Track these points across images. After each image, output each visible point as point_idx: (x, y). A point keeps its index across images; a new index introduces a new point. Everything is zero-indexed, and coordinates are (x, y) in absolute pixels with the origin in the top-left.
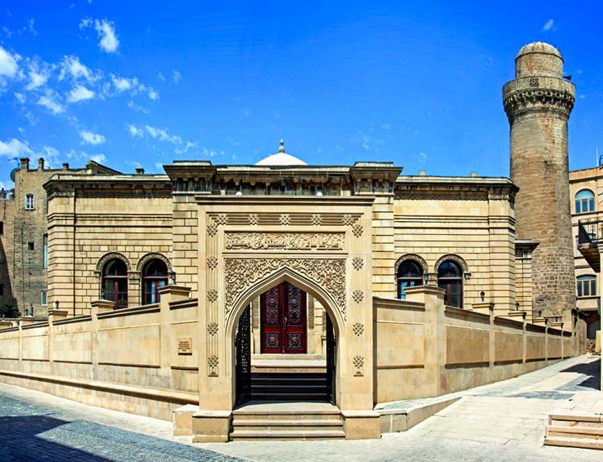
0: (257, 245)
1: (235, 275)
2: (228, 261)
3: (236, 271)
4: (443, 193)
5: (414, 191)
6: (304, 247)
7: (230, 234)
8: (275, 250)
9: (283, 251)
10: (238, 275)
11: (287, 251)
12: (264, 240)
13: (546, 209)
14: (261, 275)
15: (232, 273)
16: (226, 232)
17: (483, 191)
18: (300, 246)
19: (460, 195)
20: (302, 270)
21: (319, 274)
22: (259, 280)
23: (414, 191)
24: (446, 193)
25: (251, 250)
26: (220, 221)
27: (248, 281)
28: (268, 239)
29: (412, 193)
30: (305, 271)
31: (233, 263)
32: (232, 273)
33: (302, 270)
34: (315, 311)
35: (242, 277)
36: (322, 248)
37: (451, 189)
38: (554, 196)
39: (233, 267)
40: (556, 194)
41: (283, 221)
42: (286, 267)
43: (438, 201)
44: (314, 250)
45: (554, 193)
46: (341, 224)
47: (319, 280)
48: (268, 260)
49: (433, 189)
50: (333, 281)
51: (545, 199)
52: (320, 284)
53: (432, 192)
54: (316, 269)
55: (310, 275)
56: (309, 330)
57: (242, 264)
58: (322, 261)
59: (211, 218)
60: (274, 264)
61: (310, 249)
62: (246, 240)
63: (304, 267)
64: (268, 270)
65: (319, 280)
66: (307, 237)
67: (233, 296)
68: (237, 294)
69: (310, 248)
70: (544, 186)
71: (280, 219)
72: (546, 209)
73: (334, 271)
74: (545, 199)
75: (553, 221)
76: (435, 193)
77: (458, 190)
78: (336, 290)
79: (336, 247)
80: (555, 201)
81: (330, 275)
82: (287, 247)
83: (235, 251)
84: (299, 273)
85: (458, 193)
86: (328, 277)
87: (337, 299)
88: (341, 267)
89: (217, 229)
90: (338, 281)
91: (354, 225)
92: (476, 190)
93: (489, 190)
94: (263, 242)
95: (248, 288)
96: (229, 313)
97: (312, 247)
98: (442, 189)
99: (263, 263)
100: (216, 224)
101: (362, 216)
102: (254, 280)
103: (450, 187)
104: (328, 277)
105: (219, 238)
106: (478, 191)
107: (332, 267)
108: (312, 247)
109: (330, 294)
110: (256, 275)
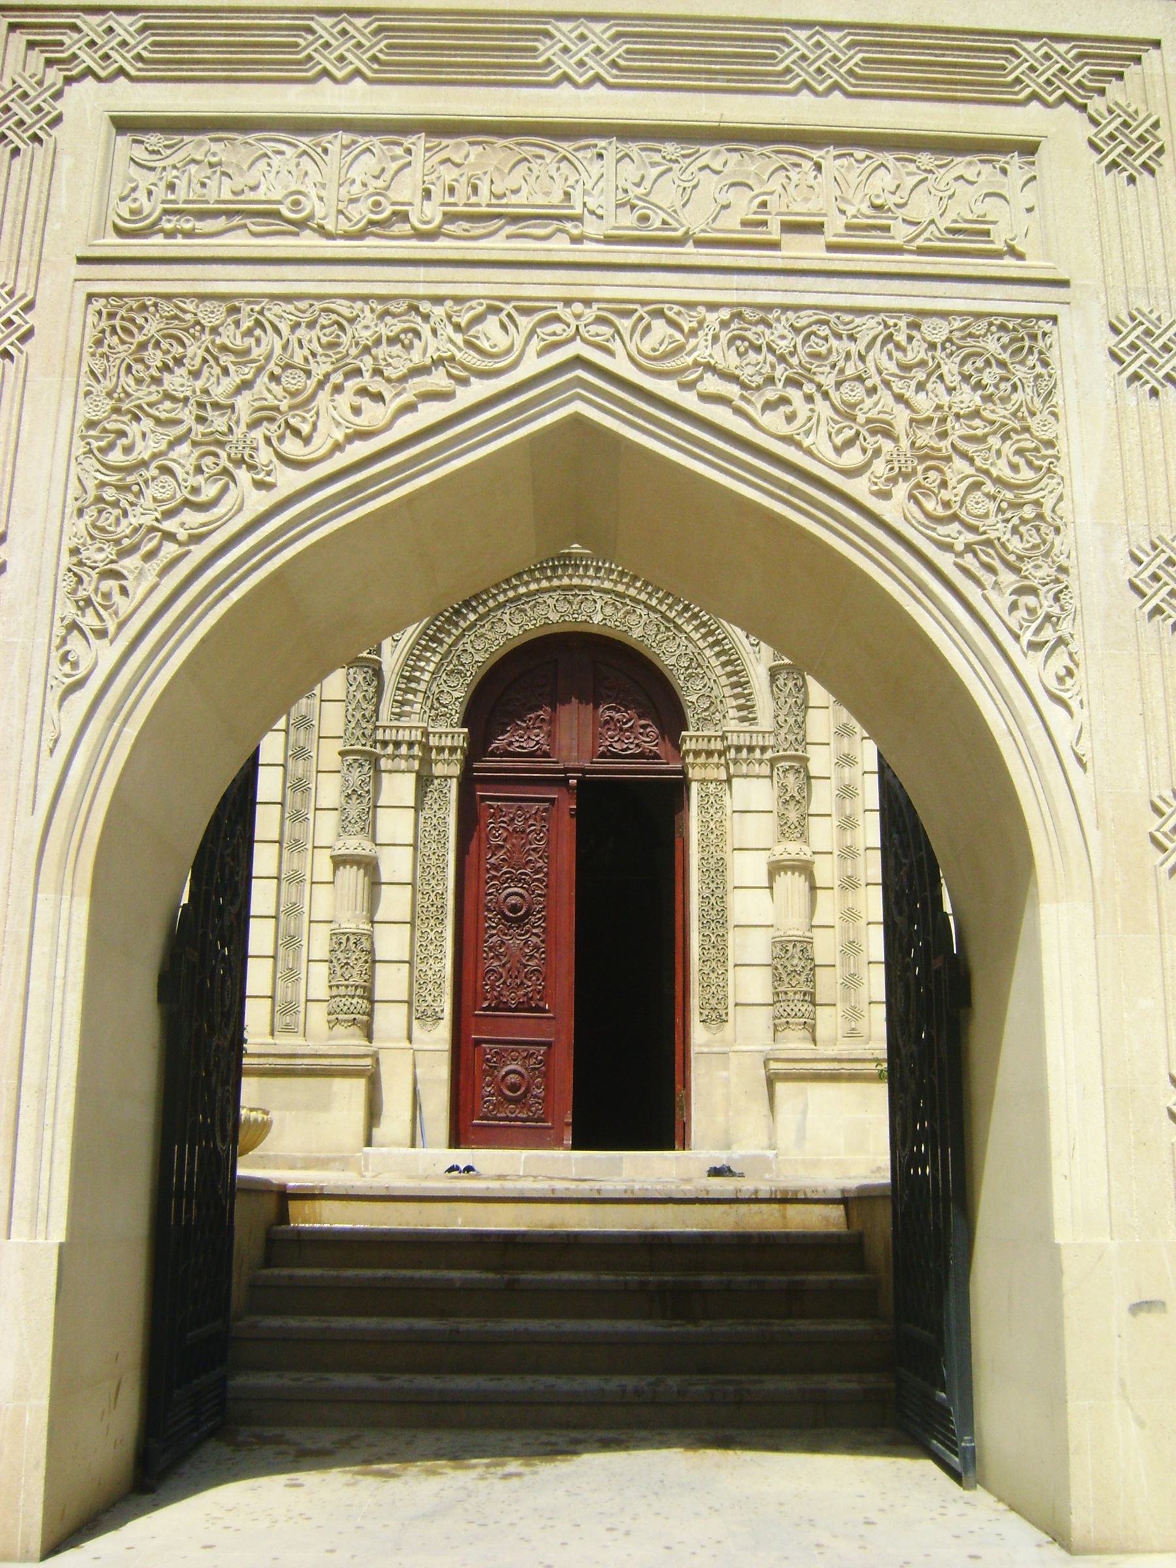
0: (361, 213)
1: (165, 410)
2: (119, 318)
3: (176, 382)
6: (730, 224)
7: (154, 140)
8: (498, 245)
9: (560, 248)
10: (188, 415)
11: (591, 252)
12: (417, 179)
14: (374, 415)
15: (145, 395)
16: (124, 125)
18: (695, 220)
20: (712, 384)
21: (847, 412)
22: (359, 450)
25: (308, 243)
26: (88, 59)
27: (264, 455)
28: (449, 174)
30: (732, 390)
31: (153, 328)
32: (145, 395)
33: (712, 384)
34: (733, 937)
35: (219, 422)
36: (868, 234)
39: (155, 358)
41: (565, 65)
42: (578, 361)
44: (805, 250)
46: (994, 90)
47: (853, 457)
48: (438, 311)
50: (959, 463)
52: (858, 488)
54: (828, 381)
55: (774, 420)
56: (699, 1035)
57: (231, 337)
58: (869, 327)
59: (19, 40)
60: (491, 333)
61: (775, 245)
62: (275, 174)
63: (729, 360)
64: (438, 380)
65: (853, 457)
66: (756, 164)
67: (129, 565)
68: (170, 550)
69: (774, 232)
71: (546, 50)
73: (968, 398)
78: (997, 530)
79: (970, 238)
81: (940, 420)
82: (592, 227)
83: (180, 247)
84: (689, 401)
86: (925, 436)
87: (1002, 602)
88: (1020, 372)
89: (60, 106)
90: (1001, 469)
91: (1096, 104)
94: (405, 191)
95: (259, 502)
96: (82, 700)
97: (790, 227)
99: (395, 326)
100: (54, 76)
101: (1151, 57)
102: (320, 445)
104: (925, 436)
105: (65, 163)
107: (950, 368)
108: (790, 227)
109: (945, 561)
110: (333, 415)
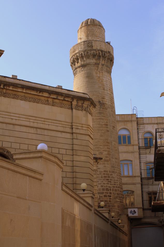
4: (33, 96)
5: (6, 89)
13: (101, 136)
17: (68, 101)
19: (48, 101)
23: (6, 89)
24: (36, 97)
29: (4, 91)
37: (41, 94)
38: (107, 127)
40: (108, 126)
43: (27, 102)
45: (107, 125)
49: (24, 91)
51: (101, 129)
53: (23, 94)
70: (100, 119)
72: (101, 136)
74: (101, 129)
75: (107, 145)
76: (26, 95)
77: (47, 96)
80: (108, 131)
85: (46, 99)
92: (62, 99)
93: (73, 100)
98: (32, 93)
103: (40, 92)
106: (64, 100)
